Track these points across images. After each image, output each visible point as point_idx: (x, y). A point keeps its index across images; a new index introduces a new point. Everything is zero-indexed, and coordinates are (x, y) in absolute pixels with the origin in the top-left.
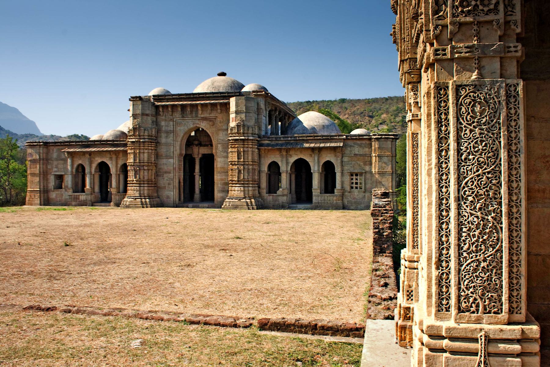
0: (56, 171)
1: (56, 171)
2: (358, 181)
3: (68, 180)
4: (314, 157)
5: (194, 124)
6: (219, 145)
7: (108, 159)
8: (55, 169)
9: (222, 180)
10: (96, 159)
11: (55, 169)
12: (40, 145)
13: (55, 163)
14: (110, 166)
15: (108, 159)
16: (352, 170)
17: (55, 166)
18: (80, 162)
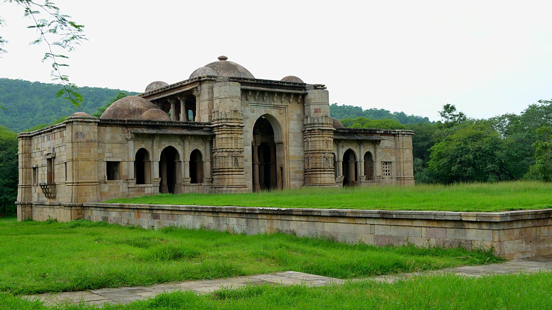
0: (110, 157)
1: (110, 157)
2: (388, 169)
3: (128, 169)
4: (360, 148)
5: (265, 111)
6: (291, 134)
7: (177, 143)
8: (108, 154)
9: (294, 168)
10: (163, 143)
11: (108, 154)
12: (95, 122)
13: (108, 146)
14: (180, 152)
15: (177, 143)
16: (384, 160)
17: (107, 151)
18: (143, 146)
